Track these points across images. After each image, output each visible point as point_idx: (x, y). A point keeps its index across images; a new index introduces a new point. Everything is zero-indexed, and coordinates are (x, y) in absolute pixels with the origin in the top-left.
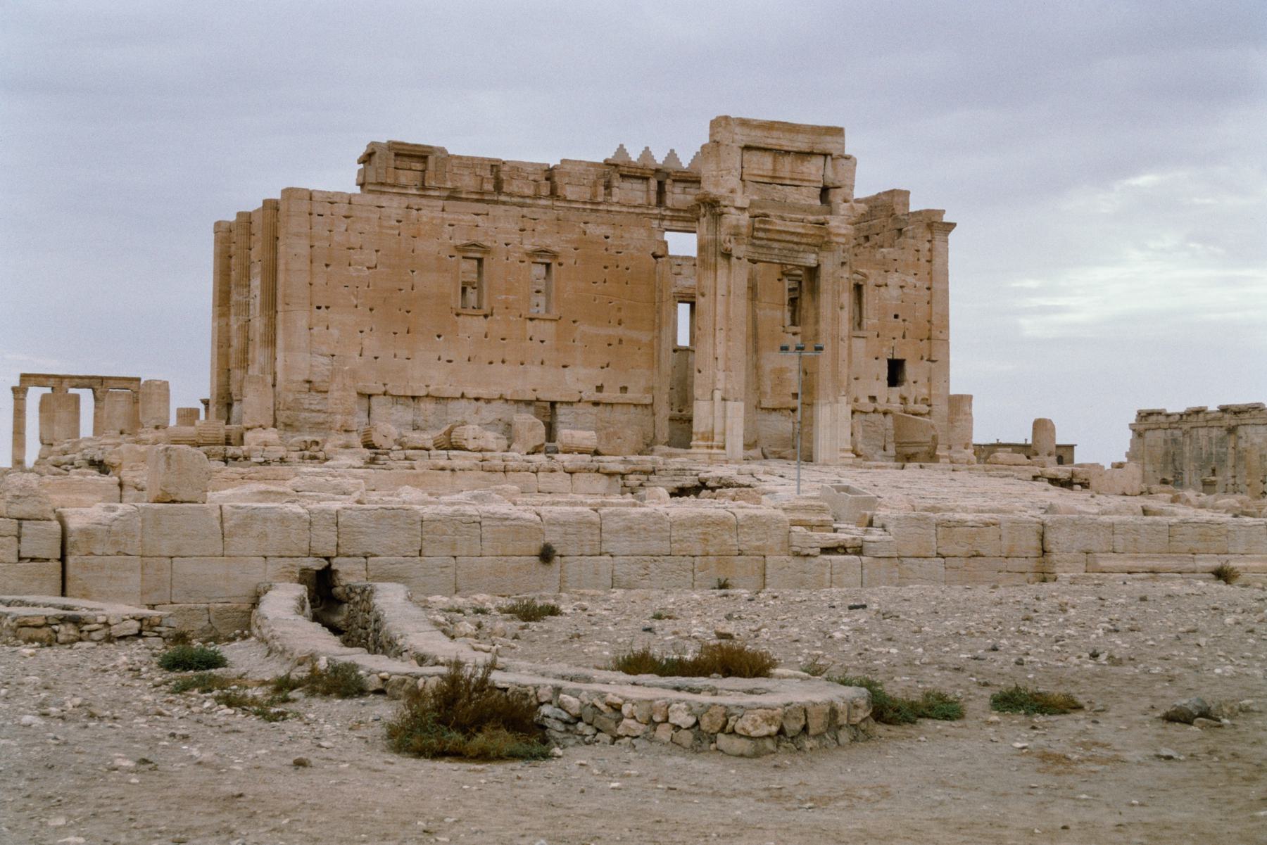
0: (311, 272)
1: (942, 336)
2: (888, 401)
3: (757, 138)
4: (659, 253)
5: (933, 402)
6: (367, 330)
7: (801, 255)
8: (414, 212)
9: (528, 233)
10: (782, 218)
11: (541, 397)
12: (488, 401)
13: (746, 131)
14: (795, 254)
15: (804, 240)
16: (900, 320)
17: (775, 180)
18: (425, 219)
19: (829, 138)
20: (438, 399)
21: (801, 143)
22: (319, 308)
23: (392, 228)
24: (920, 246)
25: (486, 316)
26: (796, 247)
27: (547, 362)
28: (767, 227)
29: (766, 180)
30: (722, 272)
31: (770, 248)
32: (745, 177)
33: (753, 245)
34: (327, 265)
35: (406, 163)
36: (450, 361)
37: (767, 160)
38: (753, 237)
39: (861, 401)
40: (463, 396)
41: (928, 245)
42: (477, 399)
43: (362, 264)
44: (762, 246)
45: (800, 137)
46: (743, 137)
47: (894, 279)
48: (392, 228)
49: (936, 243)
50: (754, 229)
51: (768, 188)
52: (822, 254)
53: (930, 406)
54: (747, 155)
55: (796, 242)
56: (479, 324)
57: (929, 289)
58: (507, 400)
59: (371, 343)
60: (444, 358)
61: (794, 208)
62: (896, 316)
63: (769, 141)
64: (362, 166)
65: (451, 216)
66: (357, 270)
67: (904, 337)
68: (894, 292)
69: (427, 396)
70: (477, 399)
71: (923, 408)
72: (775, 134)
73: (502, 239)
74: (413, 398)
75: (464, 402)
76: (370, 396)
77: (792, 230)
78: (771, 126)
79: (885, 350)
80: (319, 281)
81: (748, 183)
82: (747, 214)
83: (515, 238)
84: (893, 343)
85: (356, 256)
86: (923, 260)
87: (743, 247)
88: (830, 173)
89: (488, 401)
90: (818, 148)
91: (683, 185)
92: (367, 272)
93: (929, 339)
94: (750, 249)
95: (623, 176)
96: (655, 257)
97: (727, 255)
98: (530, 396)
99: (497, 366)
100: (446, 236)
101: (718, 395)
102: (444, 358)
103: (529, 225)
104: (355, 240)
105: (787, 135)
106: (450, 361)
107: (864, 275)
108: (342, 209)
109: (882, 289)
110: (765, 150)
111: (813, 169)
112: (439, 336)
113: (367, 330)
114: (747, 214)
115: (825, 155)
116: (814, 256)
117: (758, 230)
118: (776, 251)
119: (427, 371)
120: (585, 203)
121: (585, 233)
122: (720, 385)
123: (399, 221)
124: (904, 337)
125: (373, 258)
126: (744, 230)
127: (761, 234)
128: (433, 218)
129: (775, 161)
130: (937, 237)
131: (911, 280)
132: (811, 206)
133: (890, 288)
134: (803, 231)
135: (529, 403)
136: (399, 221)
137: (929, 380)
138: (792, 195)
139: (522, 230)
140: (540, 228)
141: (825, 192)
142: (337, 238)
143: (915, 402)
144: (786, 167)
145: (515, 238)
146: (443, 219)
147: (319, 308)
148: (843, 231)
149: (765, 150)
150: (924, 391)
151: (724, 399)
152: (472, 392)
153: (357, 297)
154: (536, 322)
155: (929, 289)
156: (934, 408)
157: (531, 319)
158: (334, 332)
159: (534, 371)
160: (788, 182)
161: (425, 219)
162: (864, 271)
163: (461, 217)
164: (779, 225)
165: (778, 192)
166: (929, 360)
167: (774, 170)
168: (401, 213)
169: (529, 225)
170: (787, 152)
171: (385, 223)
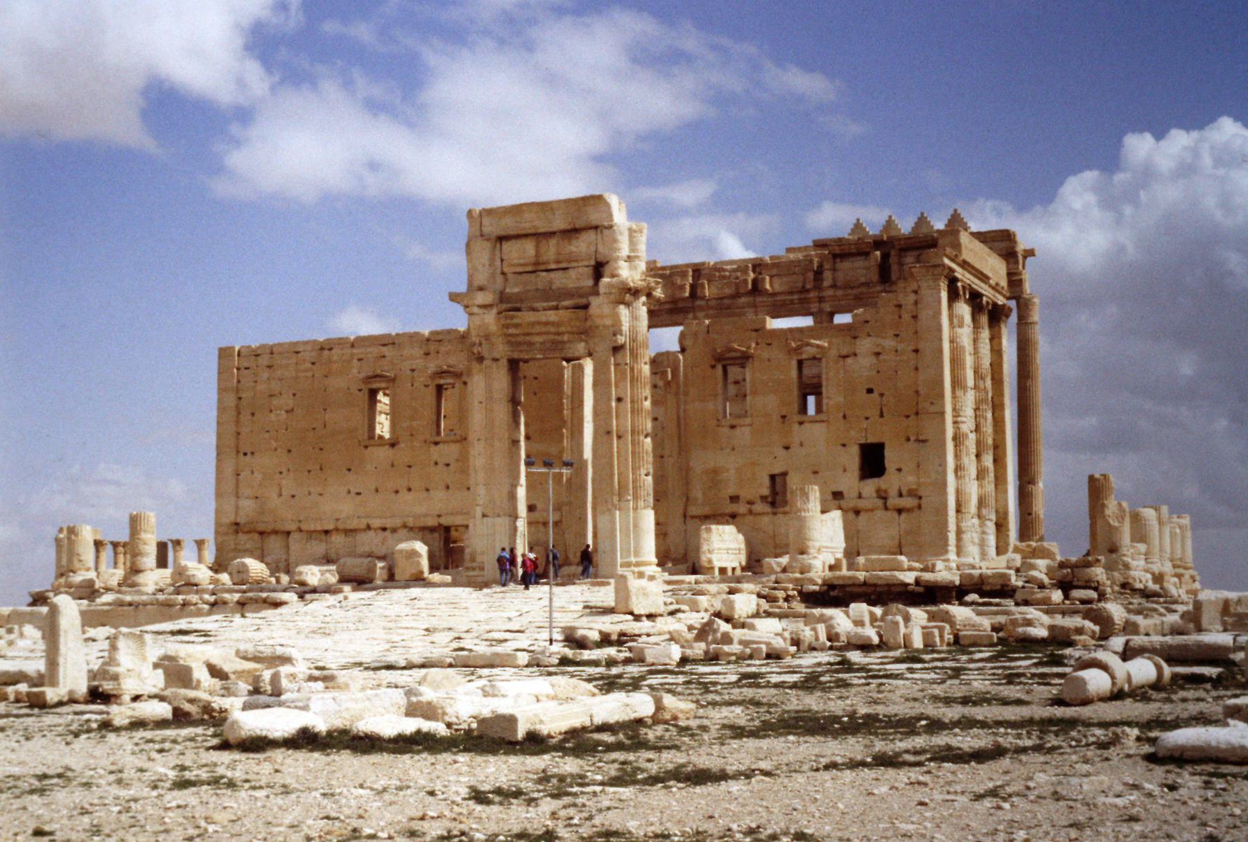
0: (237, 422)
1: (932, 409)
2: (860, 496)
3: (509, 225)
5: (920, 493)
6: (284, 470)
8: (326, 352)
9: (433, 355)
11: (445, 521)
12: (394, 530)
16: (875, 395)
17: (538, 267)
18: (335, 358)
20: (348, 532)
21: (559, 223)
23: (307, 370)
24: (901, 298)
28: (515, 321)
29: (529, 269)
31: (530, 344)
32: (505, 270)
36: (358, 494)
37: (529, 247)
40: (369, 527)
41: (912, 297)
42: (384, 529)
43: (281, 409)
46: (491, 227)
47: (865, 345)
48: (307, 370)
49: (925, 292)
51: (532, 277)
54: (507, 246)
57: (916, 351)
58: (411, 529)
59: (288, 484)
60: (353, 490)
62: (870, 391)
66: (278, 415)
67: (882, 415)
70: (384, 529)
71: (908, 502)
73: (407, 365)
74: (326, 532)
75: (371, 533)
76: (288, 533)
78: (517, 210)
79: (853, 433)
80: (245, 430)
81: (510, 276)
82: (495, 311)
83: (419, 363)
84: (865, 424)
85: (275, 402)
86: (906, 317)
88: (600, 248)
89: (394, 530)
90: (579, 224)
91: (916, 253)
93: (917, 414)
97: (480, 359)
98: (431, 522)
99: (404, 495)
100: (355, 371)
103: (432, 347)
104: (275, 386)
106: (358, 494)
107: (818, 346)
108: (264, 360)
109: (849, 361)
110: (526, 236)
111: (582, 246)
113: (284, 470)
114: (495, 311)
115: (596, 228)
116: (583, 344)
119: (336, 504)
120: (791, 293)
123: (313, 363)
124: (882, 415)
125: (291, 403)
129: (537, 247)
130: (924, 284)
131: (889, 343)
133: (860, 358)
135: (432, 530)
136: (313, 363)
138: (559, 280)
139: (427, 354)
142: (261, 387)
143: (901, 495)
144: (551, 250)
145: (419, 363)
146: (352, 354)
147: (245, 454)
149: (526, 236)
150: (910, 480)
151: (484, 516)
152: (376, 523)
153: (276, 440)
154: (441, 446)
155: (916, 351)
156: (923, 501)
157: (436, 443)
158: (258, 476)
159: (439, 495)
160: (553, 266)
163: (369, 350)
166: (918, 441)
167: (537, 255)
170: (552, 234)
171: (302, 367)
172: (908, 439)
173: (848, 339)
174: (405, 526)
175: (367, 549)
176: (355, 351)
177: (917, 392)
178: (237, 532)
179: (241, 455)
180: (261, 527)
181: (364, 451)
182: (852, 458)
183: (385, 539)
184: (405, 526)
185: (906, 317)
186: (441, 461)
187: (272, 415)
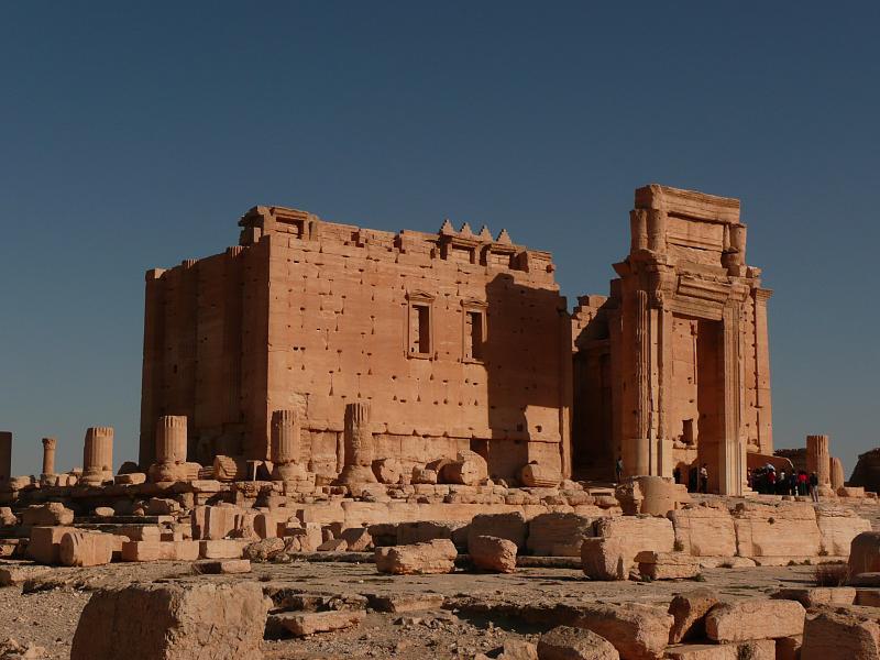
4: (561, 307)
7: (711, 310)
10: (699, 276)
13: (670, 199)
14: (706, 309)
15: (715, 297)
17: (688, 244)
18: (381, 270)
22: (296, 349)
25: (431, 360)
26: (706, 302)
27: (479, 404)
30: (654, 323)
33: (677, 299)
34: (302, 309)
35: (285, 226)
38: (678, 293)
40: (415, 434)
42: (425, 436)
43: (331, 309)
45: (709, 206)
48: (355, 277)
50: (679, 285)
53: (759, 446)
55: (706, 297)
56: (423, 366)
61: (704, 268)
63: (688, 209)
64: (243, 228)
65: (405, 268)
69: (387, 433)
70: (425, 436)
72: (691, 203)
73: (443, 289)
77: (707, 287)
85: (326, 301)
86: (749, 322)
90: (721, 218)
92: (336, 316)
94: (674, 302)
95: (455, 247)
96: (559, 311)
101: (654, 433)
102: (399, 398)
103: (463, 278)
104: (325, 286)
112: (394, 378)
116: (719, 311)
117: (683, 286)
121: (506, 288)
122: (655, 424)
123: (361, 270)
125: (340, 305)
126: (671, 286)
128: (388, 269)
132: (715, 267)
136: (361, 270)
137: (757, 424)
139: (459, 283)
140: (471, 281)
141: (727, 257)
142: (311, 283)
146: (396, 270)
147: (296, 349)
153: (327, 340)
158: (309, 372)
161: (381, 270)
164: (698, 283)
165: (691, 254)
168: (362, 263)
169: (463, 278)
174: (445, 435)
175: (413, 455)
176: (397, 266)
177: (756, 374)
180: (316, 424)
184: (445, 435)
186: (472, 381)
187: (322, 313)
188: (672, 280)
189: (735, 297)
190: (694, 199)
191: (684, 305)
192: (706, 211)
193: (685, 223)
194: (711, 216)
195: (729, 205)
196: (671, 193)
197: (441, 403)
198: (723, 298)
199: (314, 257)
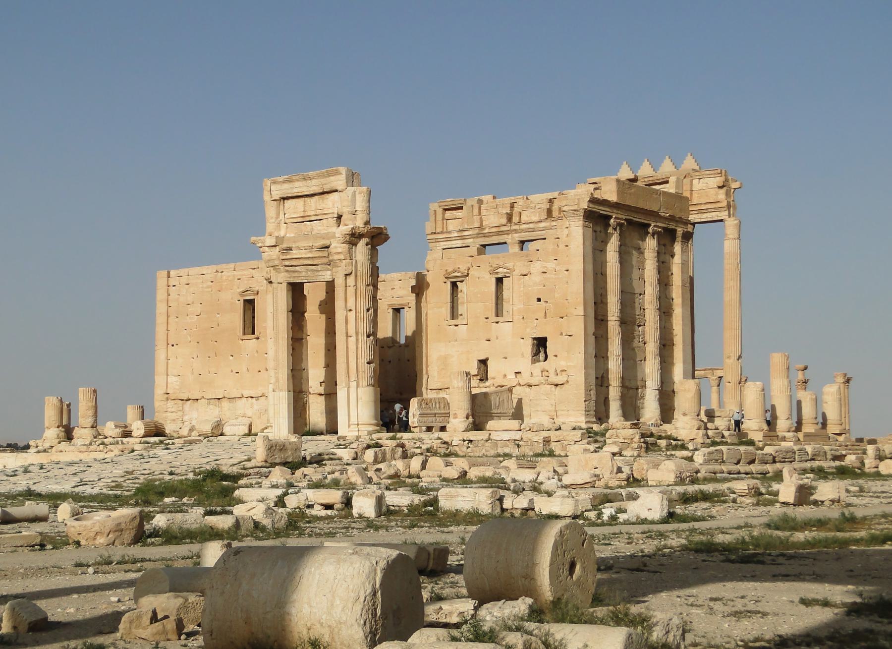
7: (320, 273)
13: (278, 187)
15: (316, 262)
18: (224, 278)
19: (332, 178)
23: (208, 287)
33: (287, 271)
39: (508, 377)
41: (566, 231)
44: (293, 272)
47: (536, 267)
48: (208, 287)
52: (334, 270)
60: (235, 371)
62: (539, 300)
68: (536, 278)
71: (560, 379)
72: (297, 184)
75: (244, 400)
79: (528, 330)
85: (190, 309)
87: (283, 274)
94: (287, 274)
100: (235, 287)
104: (190, 299)
105: (304, 182)
113: (195, 357)
116: (329, 273)
118: (304, 274)
125: (197, 308)
127: (287, 263)
131: (551, 265)
134: (310, 255)
148: (340, 250)
152: (247, 393)
153: (191, 336)
161: (224, 278)
162: (510, 265)
163: (245, 272)
172: (562, 334)
173: (527, 263)
176: (235, 273)
178: (167, 399)
179: (170, 346)
181: (241, 342)
182: (527, 347)
183: (252, 404)
185: (562, 246)
188: (274, 257)
189: (336, 257)
190: (298, 180)
191: (296, 275)
192: (313, 186)
193: (300, 202)
194: (317, 190)
195: (329, 175)
196: (275, 182)
197: (263, 371)
198: (325, 261)
199: (184, 280)
